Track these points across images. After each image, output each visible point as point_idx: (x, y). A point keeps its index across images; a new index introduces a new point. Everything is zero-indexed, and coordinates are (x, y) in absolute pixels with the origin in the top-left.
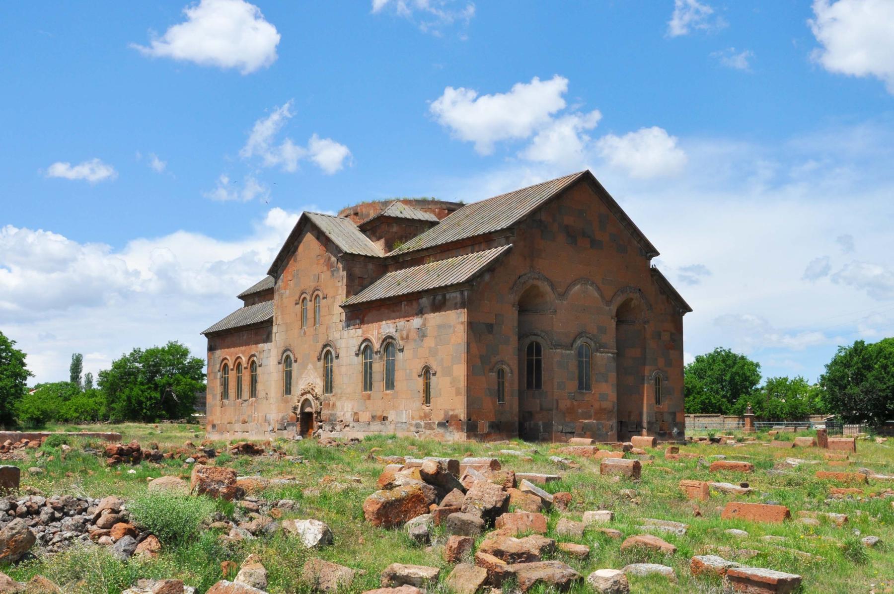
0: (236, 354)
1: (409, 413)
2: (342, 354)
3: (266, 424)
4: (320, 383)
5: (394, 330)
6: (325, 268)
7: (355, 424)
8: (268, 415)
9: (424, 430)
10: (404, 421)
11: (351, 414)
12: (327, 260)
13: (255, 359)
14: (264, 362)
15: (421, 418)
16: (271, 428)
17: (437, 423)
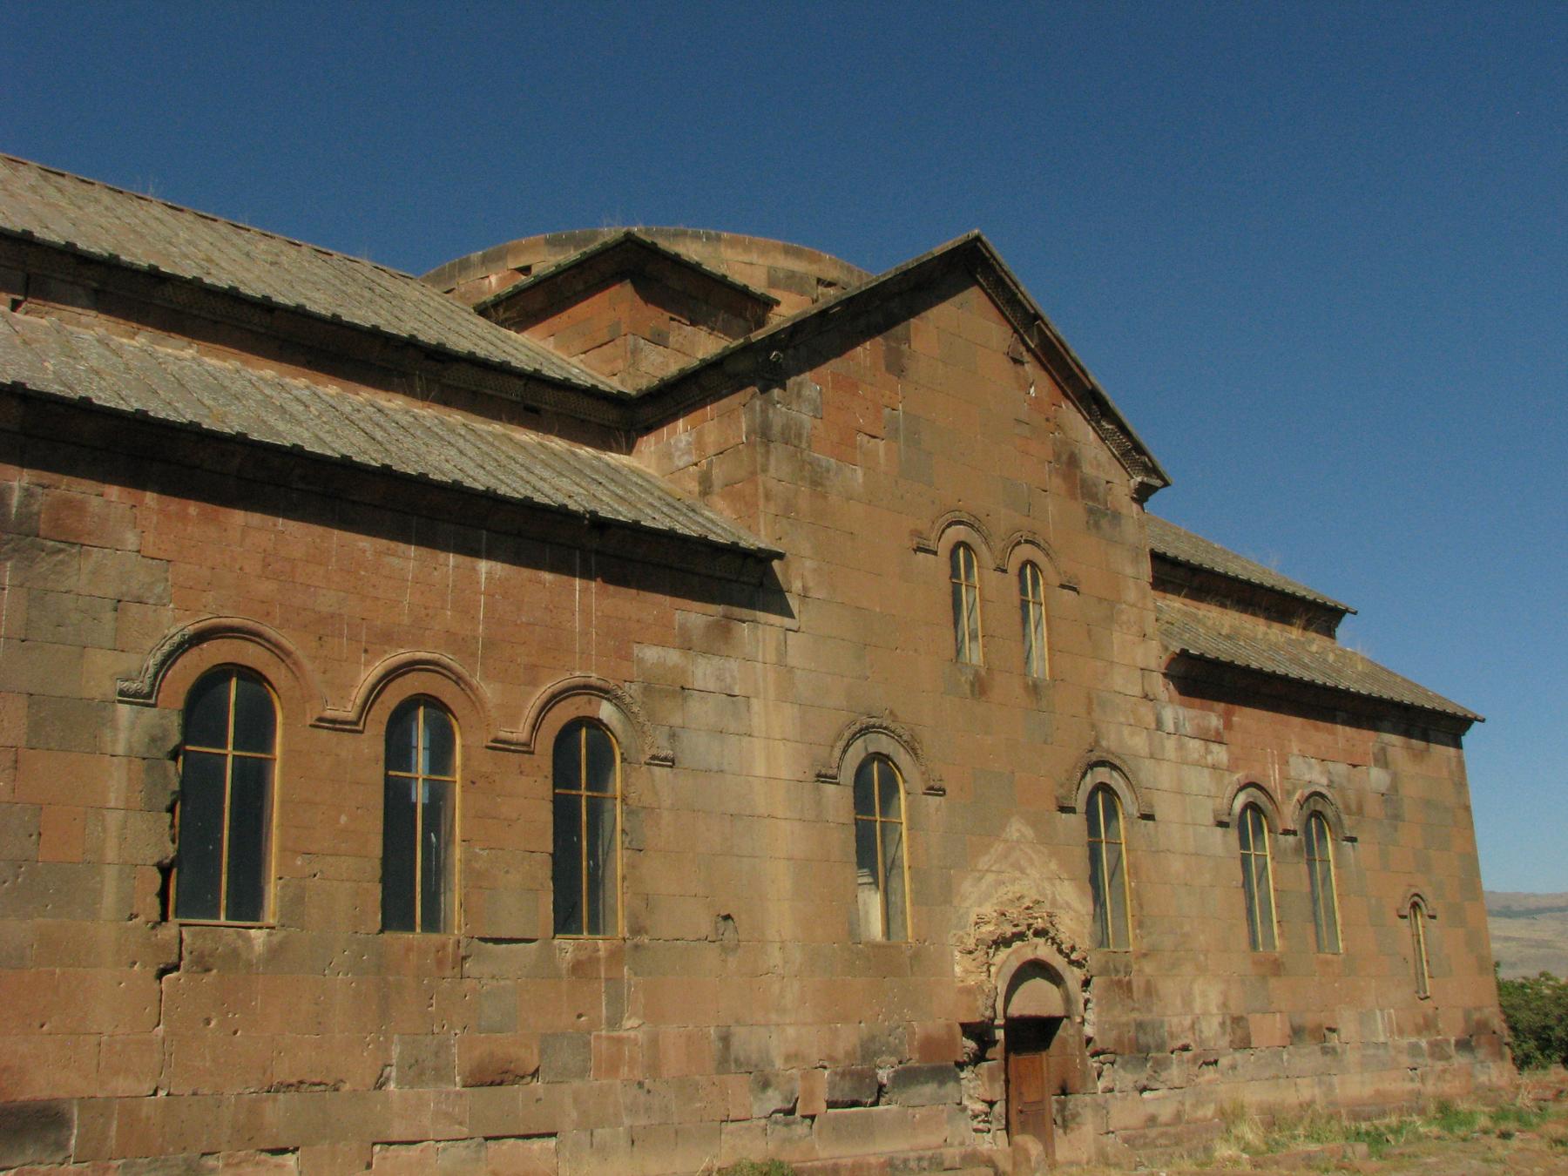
0: (388, 638)
1: (1389, 1014)
2: (1165, 809)
3: (737, 1085)
4: (1076, 904)
5: (1324, 781)
6: (1056, 483)
7: (1238, 1055)
8: (740, 1033)
9: (1429, 1061)
10: (1382, 1039)
11: (1223, 1024)
12: (1064, 458)
13: (606, 712)
14: (698, 747)
15: (1419, 1031)
16: (774, 1100)
17: (1453, 1041)
